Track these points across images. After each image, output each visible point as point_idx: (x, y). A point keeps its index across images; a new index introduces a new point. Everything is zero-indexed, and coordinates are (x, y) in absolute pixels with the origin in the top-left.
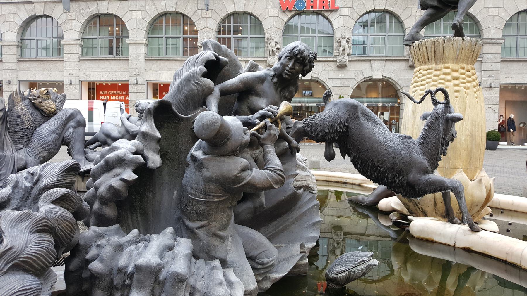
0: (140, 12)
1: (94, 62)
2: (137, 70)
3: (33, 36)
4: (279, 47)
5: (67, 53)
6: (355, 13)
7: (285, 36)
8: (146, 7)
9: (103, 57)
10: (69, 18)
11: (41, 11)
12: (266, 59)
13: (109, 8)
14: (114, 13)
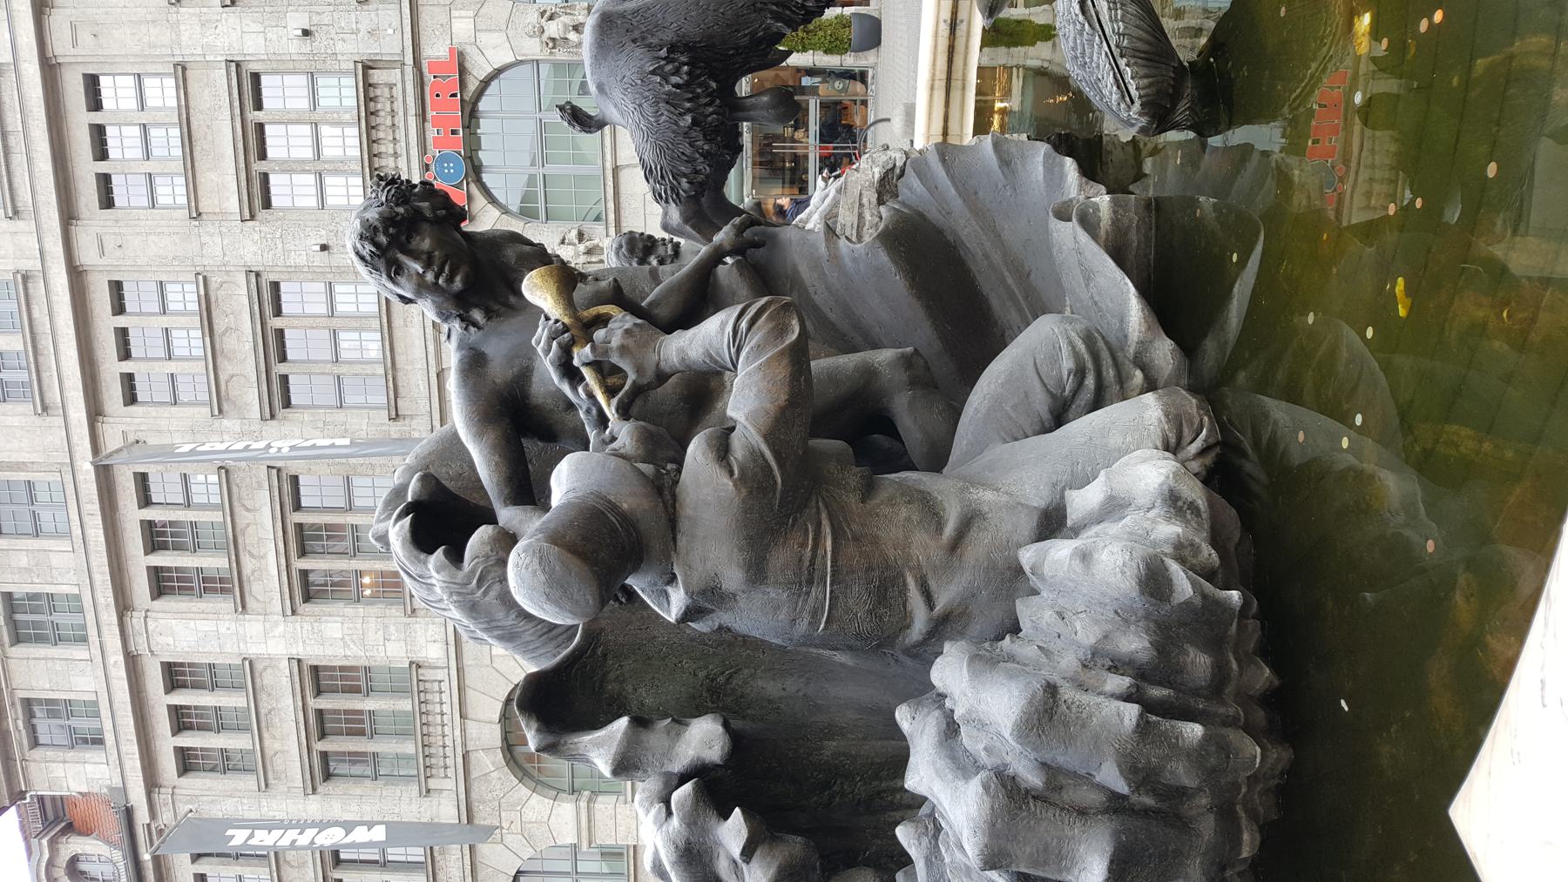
4: (574, 233)
5: (613, 834)
7: (542, 215)
10: (516, 827)
13: (486, 719)
14: (499, 706)
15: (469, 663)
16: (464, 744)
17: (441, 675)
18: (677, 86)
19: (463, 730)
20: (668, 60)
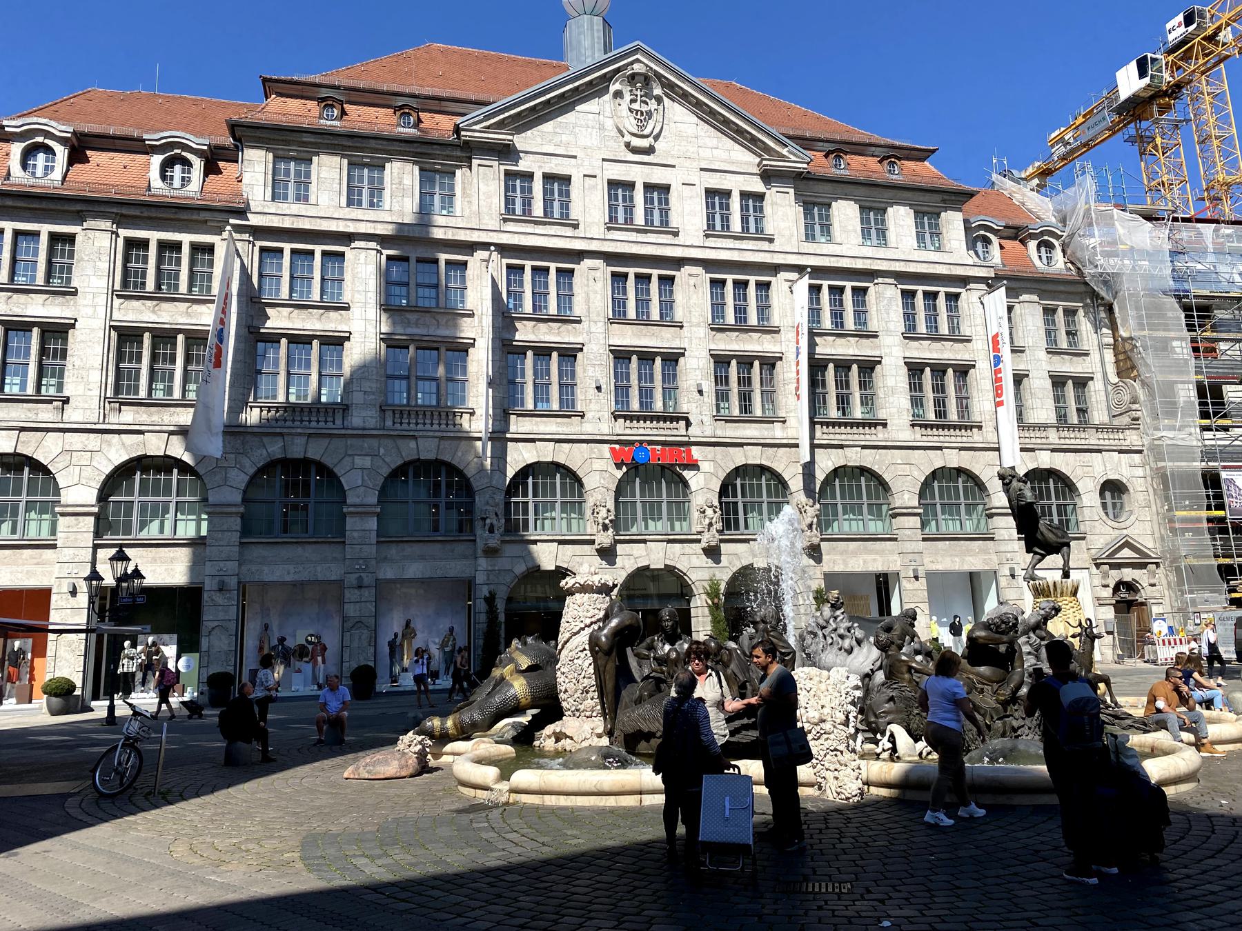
0: (369, 458)
2: (361, 562)
6: (720, 469)
8: (382, 451)
11: (159, 449)
12: (593, 537)
14: (317, 457)
15: (349, 442)
16: (289, 434)
17: (339, 422)
19: (300, 434)
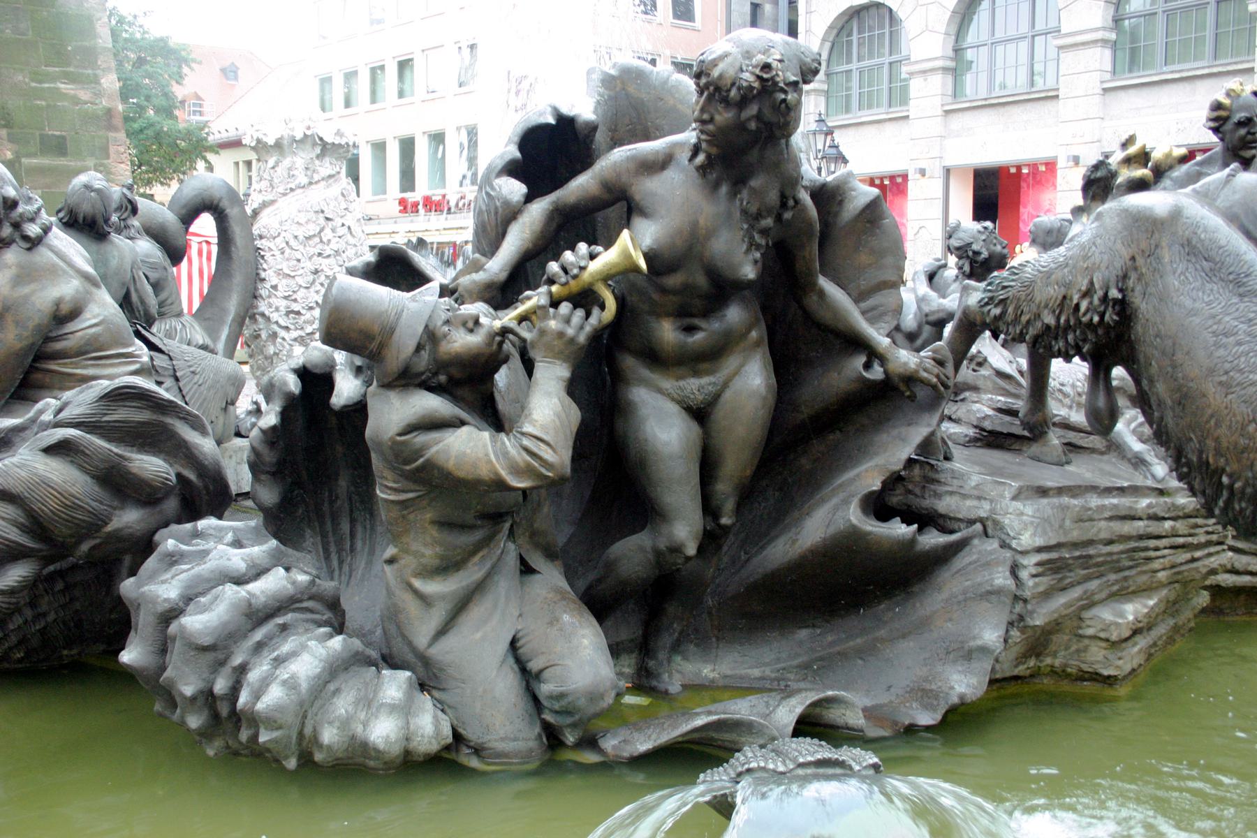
1: (1145, 92)
3: (984, 36)
9: (1172, 72)
18: (1077, 307)
20: (1105, 298)
